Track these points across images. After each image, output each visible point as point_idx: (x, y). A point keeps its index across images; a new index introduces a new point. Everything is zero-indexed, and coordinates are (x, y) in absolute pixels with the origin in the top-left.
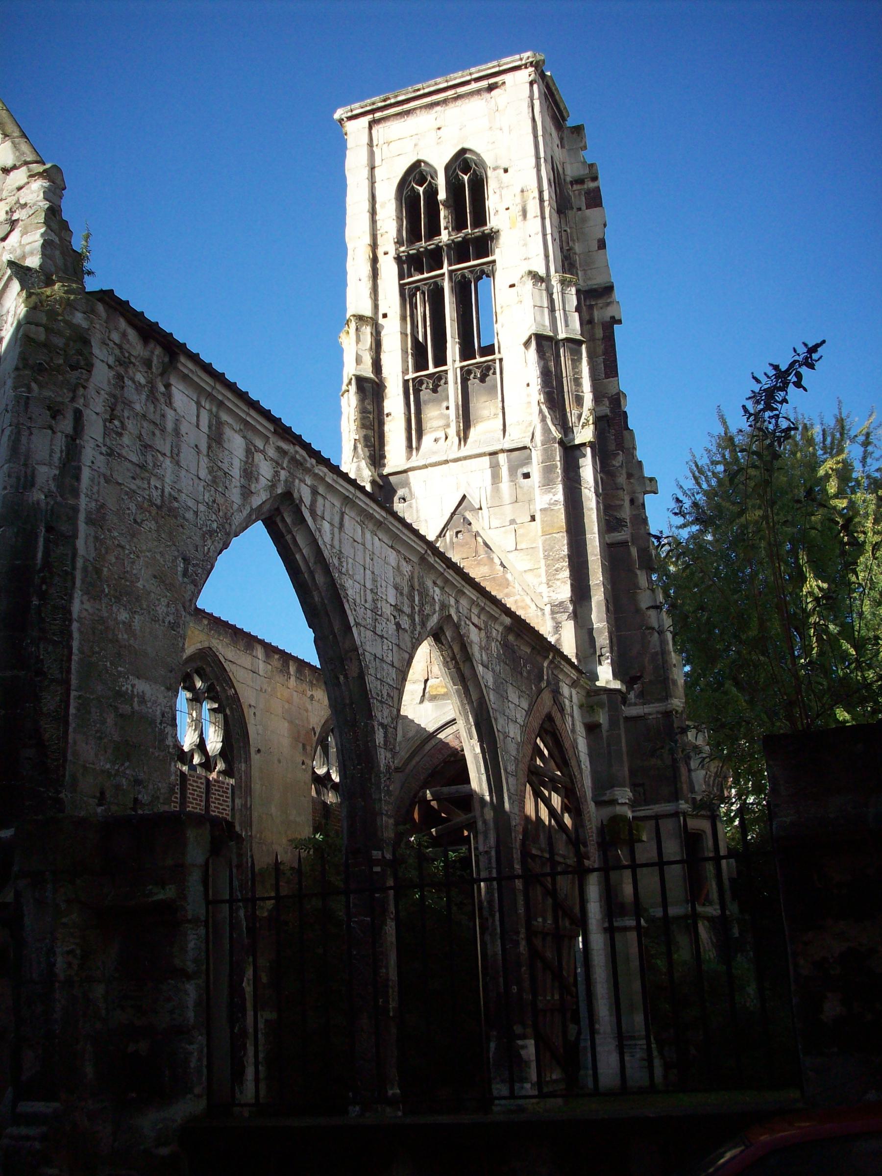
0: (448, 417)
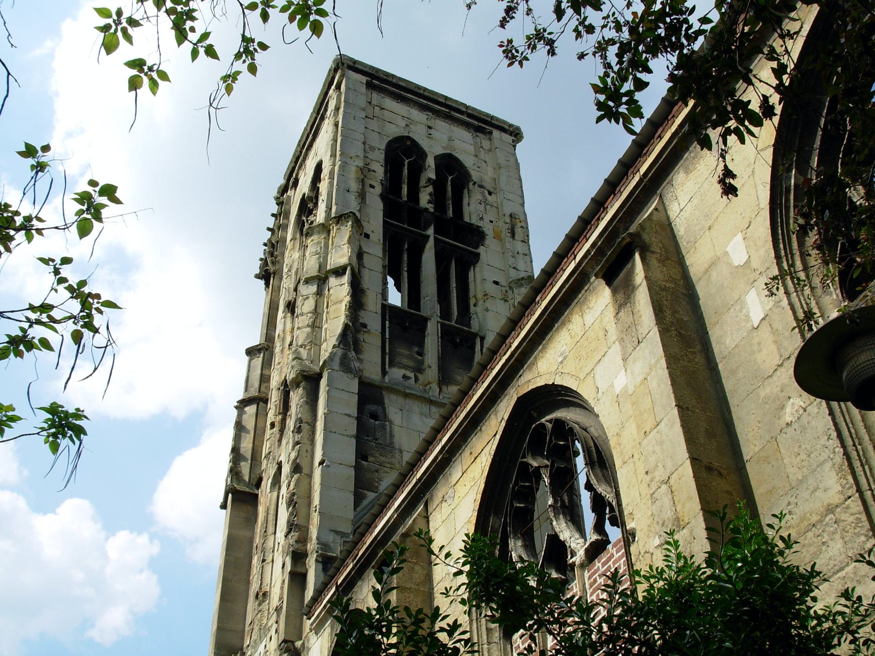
0: (422, 363)
